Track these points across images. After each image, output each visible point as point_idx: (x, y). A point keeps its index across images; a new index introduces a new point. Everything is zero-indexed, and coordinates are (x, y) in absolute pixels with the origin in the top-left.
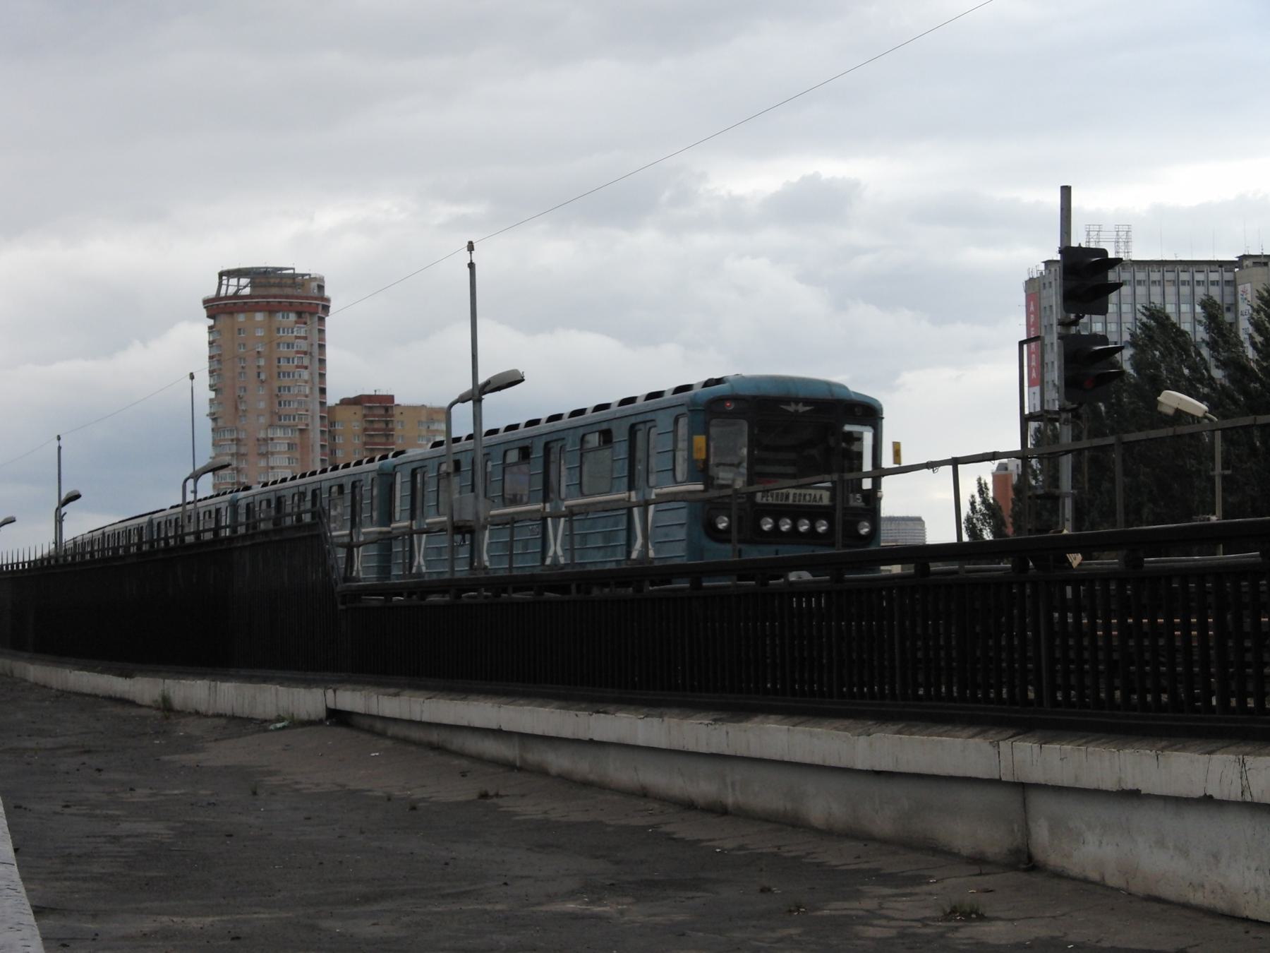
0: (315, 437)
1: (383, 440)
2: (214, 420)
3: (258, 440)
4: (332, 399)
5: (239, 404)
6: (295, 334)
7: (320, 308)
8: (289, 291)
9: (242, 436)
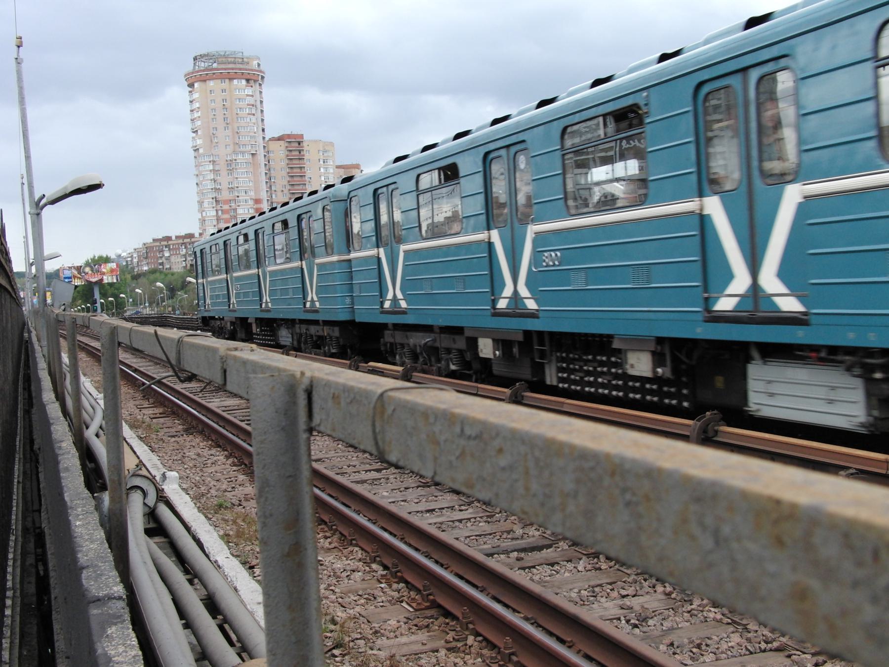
0: (262, 160)
3: (227, 161)
4: (268, 136)
5: (213, 138)
6: (246, 93)
7: (260, 77)
8: (241, 66)
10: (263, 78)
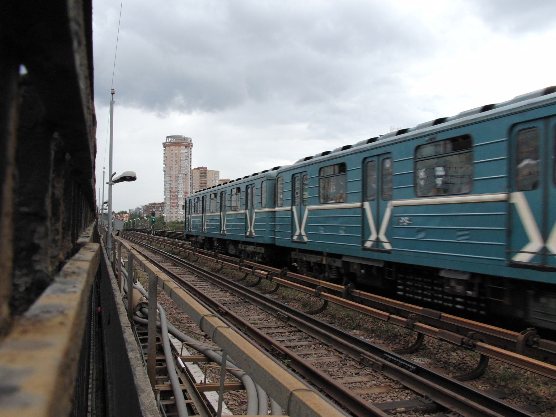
1: (204, 178)
2: (165, 172)
8: (184, 141)
9: (172, 176)
10: (192, 146)
